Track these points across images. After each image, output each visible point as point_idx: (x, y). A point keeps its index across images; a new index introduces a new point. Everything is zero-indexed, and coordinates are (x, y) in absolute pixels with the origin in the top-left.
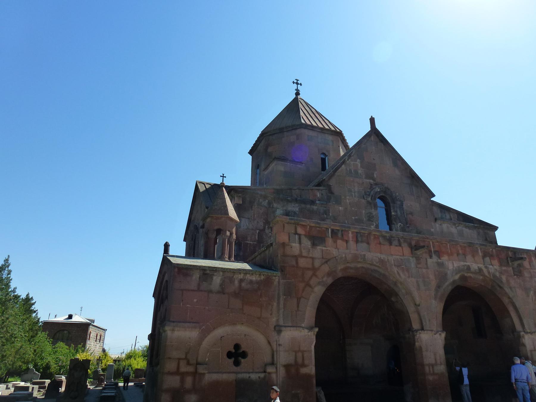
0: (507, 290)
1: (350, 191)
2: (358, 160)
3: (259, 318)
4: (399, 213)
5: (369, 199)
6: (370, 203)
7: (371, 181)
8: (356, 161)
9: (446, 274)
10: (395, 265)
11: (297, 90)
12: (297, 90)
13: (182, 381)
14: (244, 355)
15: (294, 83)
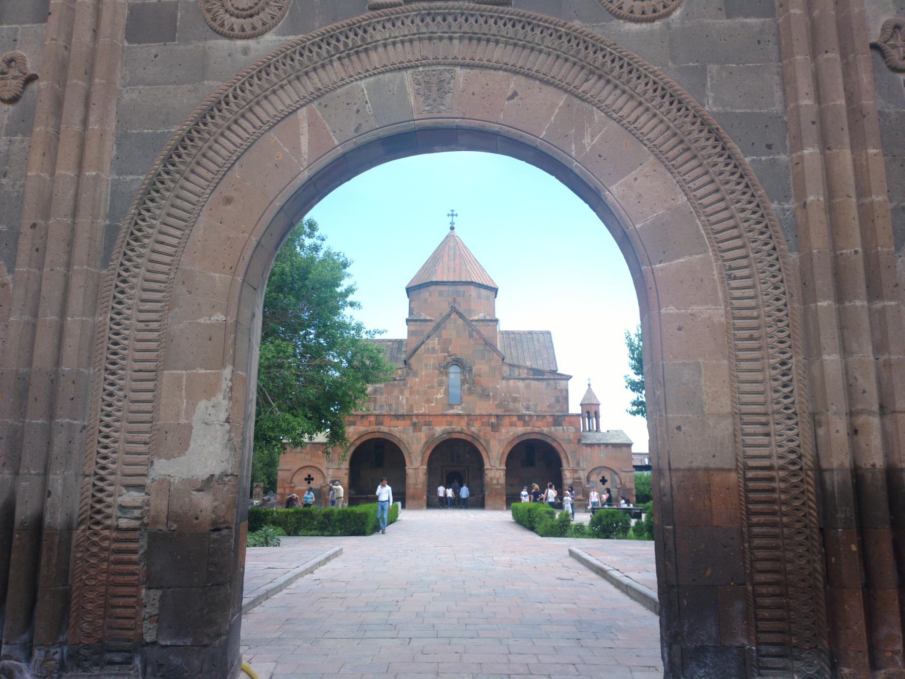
0: (483, 443)
1: (426, 365)
2: (437, 339)
3: (319, 463)
4: (468, 376)
5: (442, 369)
6: (443, 372)
7: (446, 354)
8: (434, 339)
9: (434, 434)
10: (398, 432)
11: (452, 223)
12: (452, 223)
13: (285, 490)
14: (312, 479)
15: (448, 215)
